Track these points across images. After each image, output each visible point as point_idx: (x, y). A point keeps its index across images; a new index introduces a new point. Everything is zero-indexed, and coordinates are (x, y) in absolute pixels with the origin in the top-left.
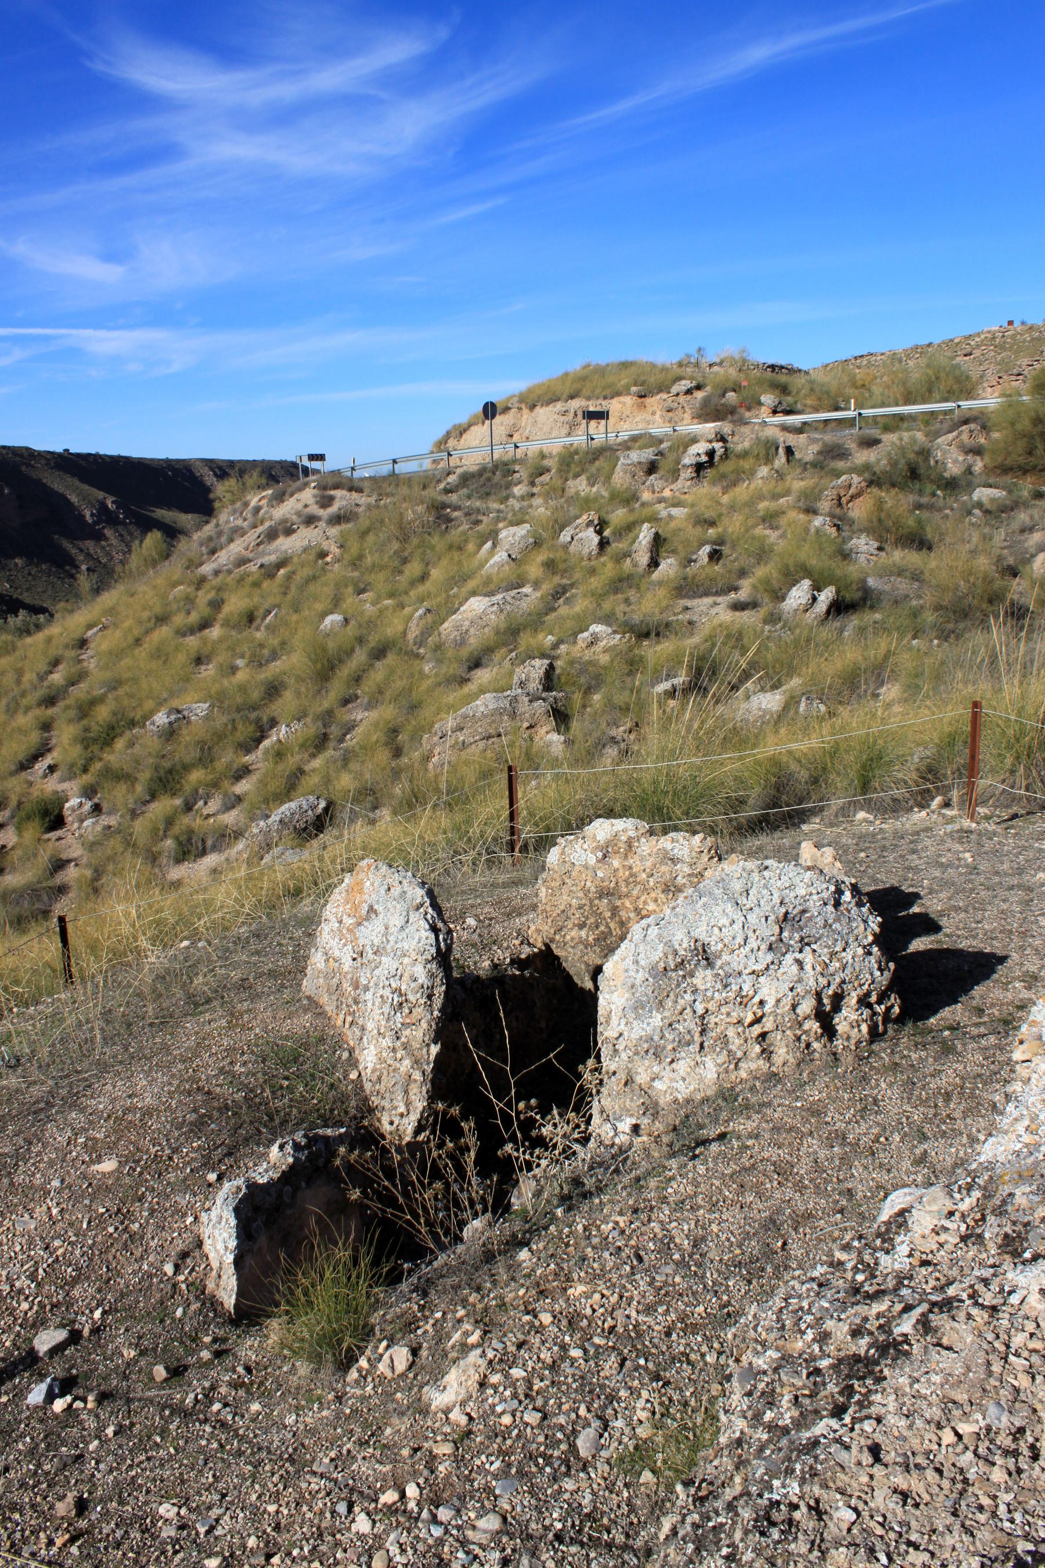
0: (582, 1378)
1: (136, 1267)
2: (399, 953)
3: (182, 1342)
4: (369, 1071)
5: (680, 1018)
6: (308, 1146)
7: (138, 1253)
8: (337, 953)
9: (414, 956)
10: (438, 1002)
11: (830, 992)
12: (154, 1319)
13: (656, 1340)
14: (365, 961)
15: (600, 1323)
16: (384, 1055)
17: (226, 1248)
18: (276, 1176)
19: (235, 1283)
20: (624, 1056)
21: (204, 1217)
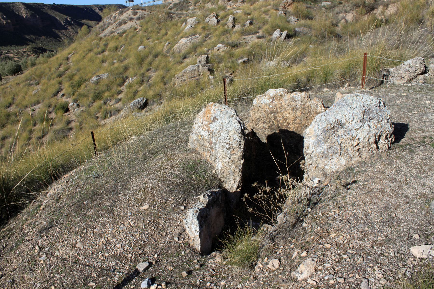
0: (351, 265)
1: (164, 239)
2: (227, 131)
3: (187, 263)
4: (219, 170)
5: (333, 145)
6: (211, 195)
7: (164, 234)
8: (202, 134)
9: (234, 132)
10: (242, 146)
11: (378, 135)
12: (175, 256)
13: (370, 250)
14: (214, 135)
15: (348, 246)
16: (225, 164)
17: (196, 231)
18: (205, 206)
19: (200, 242)
20: (314, 159)
21: (184, 221)
